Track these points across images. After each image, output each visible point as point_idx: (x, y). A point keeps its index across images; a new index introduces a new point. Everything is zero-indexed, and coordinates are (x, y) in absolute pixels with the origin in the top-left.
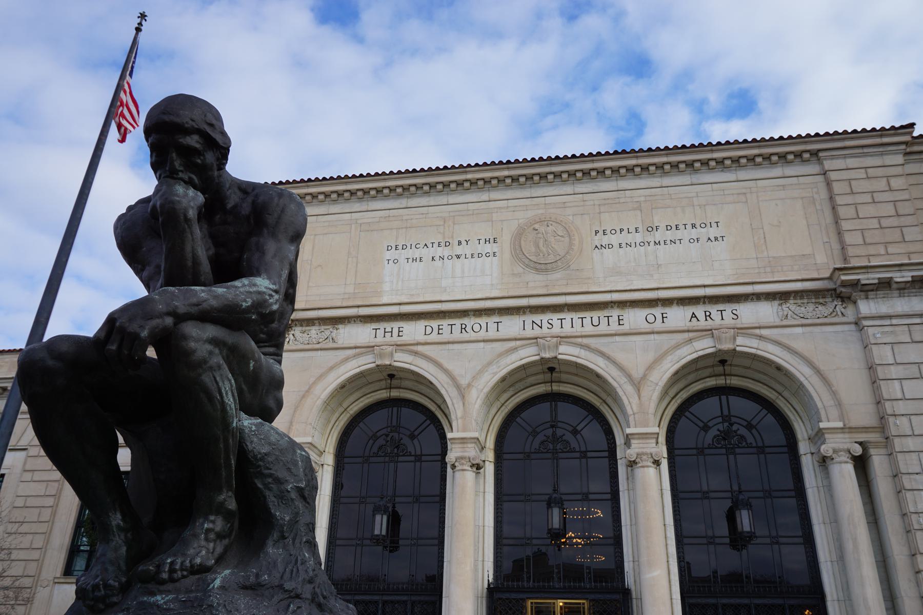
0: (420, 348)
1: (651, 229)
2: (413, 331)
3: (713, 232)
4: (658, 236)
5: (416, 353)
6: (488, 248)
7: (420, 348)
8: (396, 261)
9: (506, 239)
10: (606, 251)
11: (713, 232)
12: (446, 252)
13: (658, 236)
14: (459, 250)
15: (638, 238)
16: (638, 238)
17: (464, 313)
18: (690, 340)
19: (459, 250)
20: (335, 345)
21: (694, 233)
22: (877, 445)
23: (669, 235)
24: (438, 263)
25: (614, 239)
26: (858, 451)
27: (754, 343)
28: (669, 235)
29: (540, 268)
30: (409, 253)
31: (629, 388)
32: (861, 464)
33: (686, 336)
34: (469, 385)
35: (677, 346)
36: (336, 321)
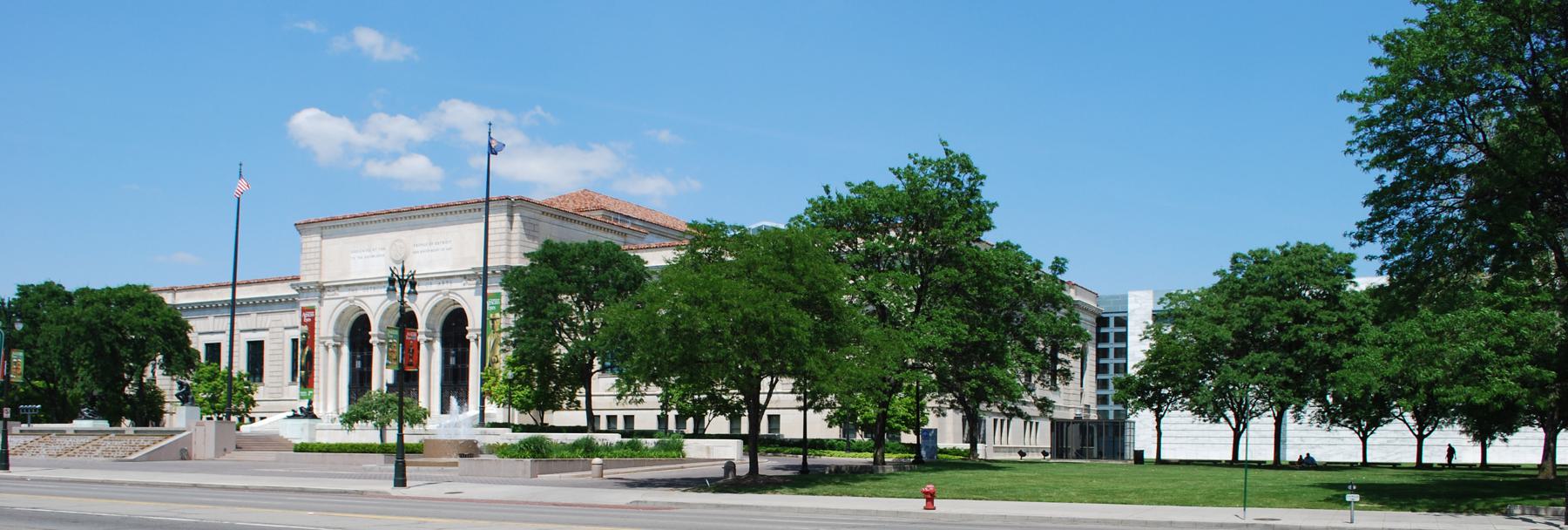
1: (431, 244)
2: (360, 292)
3: (448, 246)
6: (382, 252)
9: (387, 248)
11: (448, 246)
12: (368, 254)
18: (437, 295)
19: (374, 253)
21: (443, 246)
25: (419, 249)
27: (454, 296)
30: (358, 254)
33: (435, 293)
35: (433, 297)
36: (337, 287)
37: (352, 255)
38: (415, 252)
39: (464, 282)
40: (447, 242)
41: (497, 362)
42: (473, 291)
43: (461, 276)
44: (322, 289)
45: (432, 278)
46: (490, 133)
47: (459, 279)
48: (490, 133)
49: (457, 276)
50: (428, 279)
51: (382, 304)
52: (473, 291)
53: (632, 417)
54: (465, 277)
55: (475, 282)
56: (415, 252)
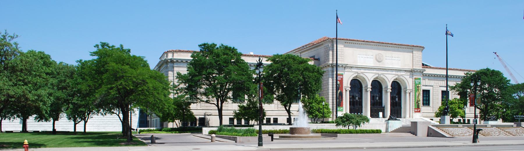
0: (364, 73)
1: (392, 57)
2: (362, 71)
4: (393, 58)
5: (363, 74)
7: (364, 73)
8: (359, 57)
10: (387, 60)
11: (399, 59)
12: (365, 56)
13: (393, 58)
14: (368, 56)
15: (391, 58)
16: (391, 58)
17: (369, 68)
19: (368, 56)
20: (351, 71)
21: (397, 59)
22: (412, 91)
23: (394, 59)
24: (365, 58)
25: (388, 58)
26: (410, 92)
28: (394, 59)
29: (379, 62)
31: (388, 82)
32: (409, 93)
34: (370, 80)
36: (352, 67)
37: (359, 56)
38: (386, 59)
39: (406, 73)
40: (399, 58)
41: (420, 101)
42: (409, 76)
43: (404, 70)
44: (345, 67)
45: (393, 70)
46: (447, 28)
47: (404, 71)
48: (447, 28)
49: (403, 70)
50: (391, 70)
51: (393, 77)
52: (409, 76)
53: (277, 119)
54: (406, 71)
55: (409, 73)
56: (386, 59)
